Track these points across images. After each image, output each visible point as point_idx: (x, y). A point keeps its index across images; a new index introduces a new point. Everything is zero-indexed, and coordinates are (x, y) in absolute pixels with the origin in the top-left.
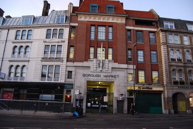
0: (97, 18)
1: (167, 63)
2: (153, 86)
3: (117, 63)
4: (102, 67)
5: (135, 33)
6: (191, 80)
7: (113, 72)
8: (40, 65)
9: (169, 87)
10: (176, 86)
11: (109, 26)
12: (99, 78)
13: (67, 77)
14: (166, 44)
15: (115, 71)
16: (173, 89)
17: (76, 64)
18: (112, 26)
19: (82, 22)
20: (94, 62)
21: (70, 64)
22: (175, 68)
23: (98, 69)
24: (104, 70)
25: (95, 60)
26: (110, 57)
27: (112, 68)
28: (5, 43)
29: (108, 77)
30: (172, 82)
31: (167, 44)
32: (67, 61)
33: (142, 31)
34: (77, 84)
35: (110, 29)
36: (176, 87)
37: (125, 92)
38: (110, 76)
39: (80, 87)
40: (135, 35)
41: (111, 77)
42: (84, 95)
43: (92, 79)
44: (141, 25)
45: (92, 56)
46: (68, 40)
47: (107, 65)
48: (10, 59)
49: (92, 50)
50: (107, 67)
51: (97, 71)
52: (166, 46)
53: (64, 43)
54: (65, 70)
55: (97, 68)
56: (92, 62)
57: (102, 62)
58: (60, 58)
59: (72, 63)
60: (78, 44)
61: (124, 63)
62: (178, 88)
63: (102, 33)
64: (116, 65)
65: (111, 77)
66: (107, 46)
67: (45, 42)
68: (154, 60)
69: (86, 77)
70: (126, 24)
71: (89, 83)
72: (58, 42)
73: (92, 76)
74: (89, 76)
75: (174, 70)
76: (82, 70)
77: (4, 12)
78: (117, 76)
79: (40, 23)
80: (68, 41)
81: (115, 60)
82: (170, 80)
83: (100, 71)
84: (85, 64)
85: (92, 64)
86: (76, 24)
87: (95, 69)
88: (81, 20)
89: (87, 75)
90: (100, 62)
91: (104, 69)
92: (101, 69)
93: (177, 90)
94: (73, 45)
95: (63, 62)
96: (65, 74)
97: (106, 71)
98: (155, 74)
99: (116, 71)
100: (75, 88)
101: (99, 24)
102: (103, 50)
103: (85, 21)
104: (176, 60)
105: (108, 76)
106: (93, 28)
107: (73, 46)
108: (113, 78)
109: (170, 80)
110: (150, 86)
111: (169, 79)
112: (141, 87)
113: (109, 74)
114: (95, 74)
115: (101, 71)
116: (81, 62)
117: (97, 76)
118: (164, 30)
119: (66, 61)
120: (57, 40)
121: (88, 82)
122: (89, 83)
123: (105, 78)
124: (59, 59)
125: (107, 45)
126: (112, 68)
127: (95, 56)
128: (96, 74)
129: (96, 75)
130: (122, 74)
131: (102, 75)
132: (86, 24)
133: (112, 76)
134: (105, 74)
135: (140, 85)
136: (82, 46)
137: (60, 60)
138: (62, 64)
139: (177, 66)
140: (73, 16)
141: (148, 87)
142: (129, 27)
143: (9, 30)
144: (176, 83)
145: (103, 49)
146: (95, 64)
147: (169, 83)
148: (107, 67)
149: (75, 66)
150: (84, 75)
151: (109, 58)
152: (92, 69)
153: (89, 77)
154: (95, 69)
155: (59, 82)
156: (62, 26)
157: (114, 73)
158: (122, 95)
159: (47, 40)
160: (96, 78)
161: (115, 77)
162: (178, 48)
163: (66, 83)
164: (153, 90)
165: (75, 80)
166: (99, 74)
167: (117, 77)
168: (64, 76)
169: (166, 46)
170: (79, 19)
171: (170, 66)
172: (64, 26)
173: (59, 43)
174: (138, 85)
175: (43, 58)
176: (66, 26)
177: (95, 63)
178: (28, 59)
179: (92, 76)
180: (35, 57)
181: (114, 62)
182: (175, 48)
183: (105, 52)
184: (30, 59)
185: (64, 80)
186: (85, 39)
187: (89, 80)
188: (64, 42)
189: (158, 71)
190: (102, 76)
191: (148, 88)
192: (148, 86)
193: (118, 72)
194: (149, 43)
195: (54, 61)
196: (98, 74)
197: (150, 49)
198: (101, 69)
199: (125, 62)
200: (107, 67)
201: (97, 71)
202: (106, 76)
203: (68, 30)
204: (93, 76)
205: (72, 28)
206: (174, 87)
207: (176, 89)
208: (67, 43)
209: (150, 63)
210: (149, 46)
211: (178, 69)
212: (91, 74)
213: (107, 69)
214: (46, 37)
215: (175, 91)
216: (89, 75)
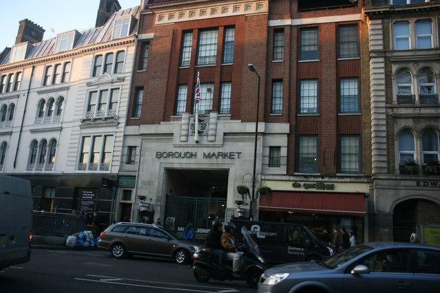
0: (198, 11)
1: (384, 111)
2: (336, 180)
4: (199, 132)
5: (295, 34)
6: (406, 159)
7: (225, 143)
8: (78, 137)
9: (385, 183)
10: (408, 178)
11: (227, 27)
12: (193, 160)
13: (125, 159)
14: (386, 53)
15: (233, 140)
16: (396, 188)
17: (145, 129)
18: (233, 27)
19: (164, 27)
21: (133, 130)
22: (410, 123)
23: (190, 138)
24: (205, 141)
25: (185, 116)
26: (226, 104)
27: (225, 134)
28: (26, 95)
29: (214, 157)
30: (397, 167)
31: (388, 55)
32: (128, 123)
33: (315, 27)
34: (143, 177)
35: (231, 36)
36: (408, 183)
38: (219, 155)
39: (149, 183)
40: (295, 41)
41: (220, 157)
42: (158, 200)
43: (177, 163)
45: (182, 107)
47: (212, 126)
48: (32, 128)
49: (183, 93)
51: (188, 143)
52: (382, 60)
54: (121, 144)
55: (187, 136)
56: (179, 122)
58: (112, 118)
62: (418, 185)
63: (208, 48)
64: (236, 126)
65: (220, 157)
67: (89, 84)
68: (348, 108)
69: (163, 160)
70: (271, 15)
71: (171, 174)
72: (112, 83)
73: (177, 155)
75: (406, 131)
77: (44, 31)
78: (236, 155)
79: (87, 45)
81: (235, 114)
82: (390, 160)
84: (163, 128)
85: (178, 127)
86: (150, 35)
87: (184, 138)
89: (165, 155)
92: (196, 137)
93: (412, 192)
94: (141, 84)
96: (120, 154)
98: (350, 145)
99: (234, 141)
100: (140, 184)
102: (209, 90)
104: (417, 99)
105: (214, 154)
106: (189, 40)
107: (142, 88)
108: (227, 161)
109: (390, 160)
110: (333, 180)
111: (385, 159)
112: (302, 183)
113: (216, 151)
114: (183, 151)
115: (197, 142)
117: (188, 155)
118: (379, 12)
120: (109, 76)
122: (171, 174)
123: (207, 161)
124: (111, 120)
125: (219, 75)
126: (225, 134)
127: (190, 109)
128: (186, 150)
129: (186, 154)
130: (247, 148)
131: (200, 152)
132: (171, 32)
133: (224, 155)
134: (207, 151)
135: (298, 179)
136: (158, 85)
137: (113, 123)
138: (118, 130)
139: (416, 118)
140: (145, 17)
141: (321, 182)
142: (279, 21)
143: (34, 67)
144: (409, 169)
147: (386, 171)
148: (211, 132)
149: (141, 135)
150: (159, 155)
153: (170, 160)
154: (184, 138)
156: (121, 44)
157: (230, 147)
159: (93, 80)
160: (185, 160)
161: (231, 156)
162: (425, 61)
163: (121, 174)
164: (337, 190)
165: (141, 167)
168: (119, 158)
169: (382, 60)
170: (157, 22)
171: (392, 119)
174: (292, 178)
175: (84, 121)
177: (185, 124)
178: (60, 126)
180: (71, 120)
182: (415, 62)
184: (64, 126)
185: (118, 168)
186: (167, 67)
187: (170, 166)
188: (123, 80)
189: (357, 135)
190: (200, 156)
191: (321, 185)
192: (320, 179)
193: (240, 144)
194: (334, 56)
195: (103, 126)
196: (190, 150)
197: (337, 74)
198: (196, 137)
199: (263, 119)
200: (211, 132)
201: (188, 143)
202: (209, 156)
205: (143, 45)
206: (403, 183)
207: (407, 188)
209: (333, 116)
210: (334, 65)
211: (423, 124)
212: (174, 150)
213: (211, 138)
214: (92, 74)
215: (404, 194)
216: (170, 155)
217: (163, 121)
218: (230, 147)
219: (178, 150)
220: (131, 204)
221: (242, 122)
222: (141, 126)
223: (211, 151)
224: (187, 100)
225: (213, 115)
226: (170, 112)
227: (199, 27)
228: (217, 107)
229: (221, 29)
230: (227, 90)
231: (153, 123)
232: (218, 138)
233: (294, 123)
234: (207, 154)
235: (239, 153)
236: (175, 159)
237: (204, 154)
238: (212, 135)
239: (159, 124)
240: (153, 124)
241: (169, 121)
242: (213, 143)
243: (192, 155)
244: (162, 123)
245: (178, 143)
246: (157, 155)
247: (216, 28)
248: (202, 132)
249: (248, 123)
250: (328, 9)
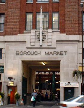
12: (39, 56)
20: (32, 34)
24: (45, 45)
25: (33, 31)
27: (57, 41)
29: (51, 54)
38: (54, 53)
49: (30, 17)
50: (50, 40)
51: (35, 47)
56: (29, 34)
57: (42, 34)
60: (9, 10)
61: (75, 34)
66: (51, 10)
69: (20, 56)
73: (29, 53)
74: (25, 54)
81: (62, 30)
83: (40, 46)
84: (20, 37)
85: (29, 36)
89: (21, 53)
90: (40, 34)
91: (46, 43)
97: (49, 46)
105: (51, 53)
108: (59, 56)
113: (52, 51)
114: (33, 51)
115: (41, 46)
116: (14, 35)
121: (24, 63)
126: (57, 41)
131: (43, 52)
134: (47, 51)
145: (45, 14)
146: (33, 37)
149: (5, 42)
150: (18, 53)
151: (53, 28)
152: (28, 45)
154: (33, 44)
157: (60, 48)
161: (61, 54)
166: (38, 51)
167: (64, 54)
179: (29, 53)
181: (61, 32)
183: (49, 19)
198: (41, 43)
201: (35, 47)
204: (31, 54)
212: (27, 50)
216: (25, 53)
217: (19, 34)
218: (60, 48)
223: (50, 51)
224: (33, 22)
225: (50, 30)
226: (22, 28)
228: (50, 26)
230: (55, 17)
231: (13, 34)
232: (53, 43)
235: (66, 52)
236: (27, 55)
237: (45, 52)
238: (50, 42)
241: (23, 33)
242: (51, 46)
243: (38, 53)
244: (18, 34)
246: (16, 53)
248: (43, 40)
249: (70, 35)
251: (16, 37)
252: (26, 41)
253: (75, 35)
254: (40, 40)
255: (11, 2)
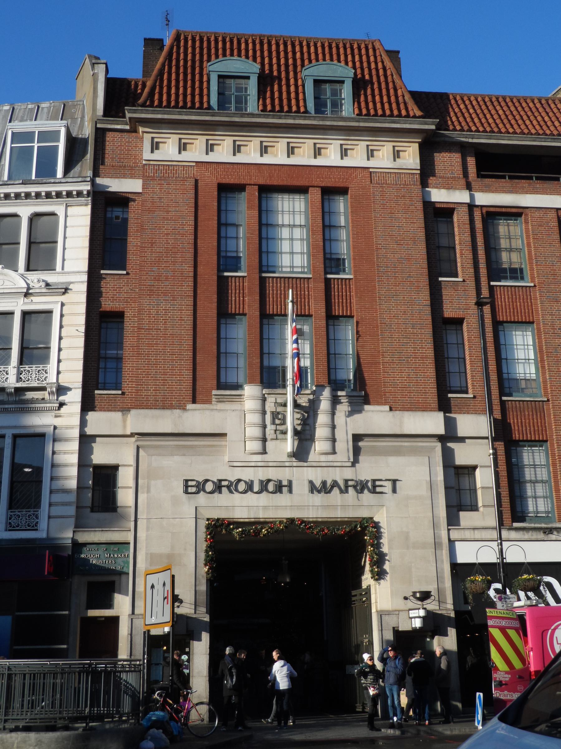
3: (385, 404)
12: (283, 499)
15: (376, 452)
18: (343, 191)
37: (439, 578)
38: (347, 487)
44: (511, 178)
46: (85, 278)
53: (63, 298)
59: (117, 416)
61: (424, 408)
69: (202, 498)
76: (177, 458)
78: (389, 485)
80: (84, 287)
83: (285, 458)
88: (157, 155)
90: (285, 405)
95: (64, 409)
101: (269, 182)
103: (184, 166)
116: (171, 407)
119: (77, 408)
123: (318, 499)
128: (261, 474)
142: (443, 191)
155: (41, 534)
156: (48, 195)
158: (425, 596)
160: (264, 499)
172: (59, 195)
173: (35, 299)
176: (69, 194)
187: (216, 514)
193: (392, 460)
196: (273, 474)
203: (87, 221)
208: (83, 298)
217: (194, 401)
219: (247, 475)
220: (115, 620)
221: (391, 409)
222: (133, 412)
227: (262, 182)
229: (315, 194)
233: (498, 415)
234: (318, 484)
237: (311, 482)
239: (184, 409)
240: (164, 408)
245: (241, 456)
246: (186, 486)
247: (302, 190)
249: (406, 414)
250: (537, 178)
251: (180, 417)
252: (224, 435)
253: (425, 413)
254: (285, 433)
255: (155, 269)
